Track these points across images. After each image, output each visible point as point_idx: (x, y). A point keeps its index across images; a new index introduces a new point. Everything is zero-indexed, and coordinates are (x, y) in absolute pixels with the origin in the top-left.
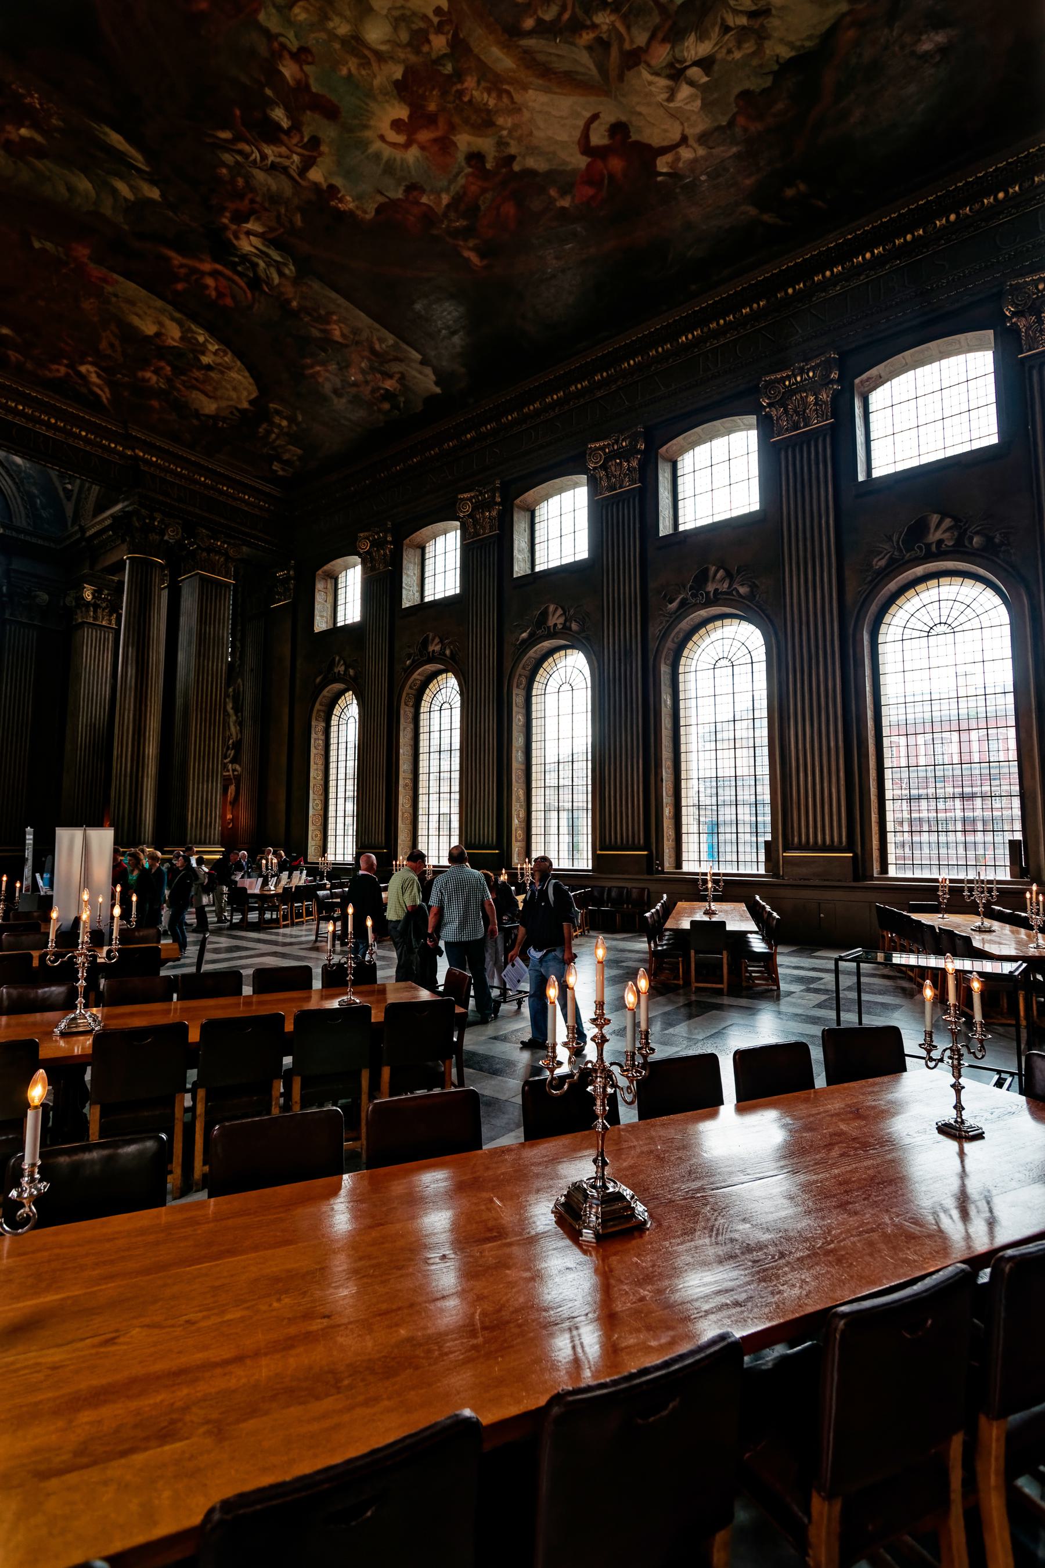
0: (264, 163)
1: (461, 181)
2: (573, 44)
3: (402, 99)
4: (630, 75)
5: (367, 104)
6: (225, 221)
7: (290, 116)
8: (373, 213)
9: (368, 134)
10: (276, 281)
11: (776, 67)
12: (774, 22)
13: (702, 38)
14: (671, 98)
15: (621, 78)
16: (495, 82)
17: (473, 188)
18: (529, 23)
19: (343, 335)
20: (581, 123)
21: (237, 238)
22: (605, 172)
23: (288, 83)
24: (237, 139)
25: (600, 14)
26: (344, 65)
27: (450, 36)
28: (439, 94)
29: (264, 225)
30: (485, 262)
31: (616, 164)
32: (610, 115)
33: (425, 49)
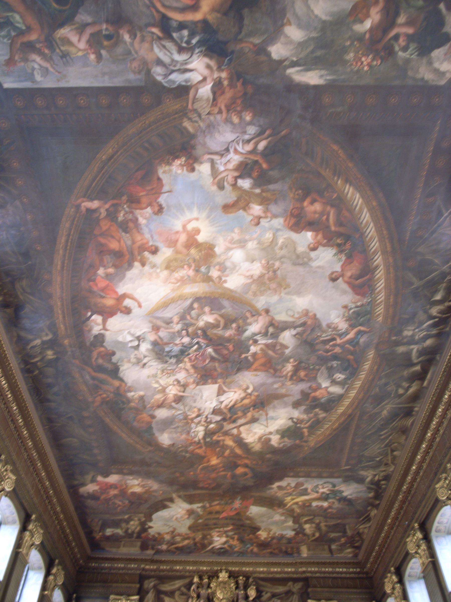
0: (233, 148)
1: (147, 236)
2: (177, 314)
3: (206, 243)
4: (150, 325)
5: (216, 227)
6: (224, 75)
7: (240, 189)
8: (161, 176)
9: (204, 215)
10: (156, 50)
11: (119, 364)
12: (137, 368)
13: (148, 350)
14: (129, 333)
15: (151, 322)
16: (183, 281)
17: (138, 238)
18: (196, 305)
19: (70, 43)
20: (141, 300)
21: (208, 67)
22: (108, 296)
23: (253, 203)
24: (254, 151)
25: (181, 327)
26: (238, 233)
27: (214, 279)
28: (196, 258)
29: (200, 100)
30: (83, 209)
31: (109, 302)
32: (136, 311)
33: (217, 267)
